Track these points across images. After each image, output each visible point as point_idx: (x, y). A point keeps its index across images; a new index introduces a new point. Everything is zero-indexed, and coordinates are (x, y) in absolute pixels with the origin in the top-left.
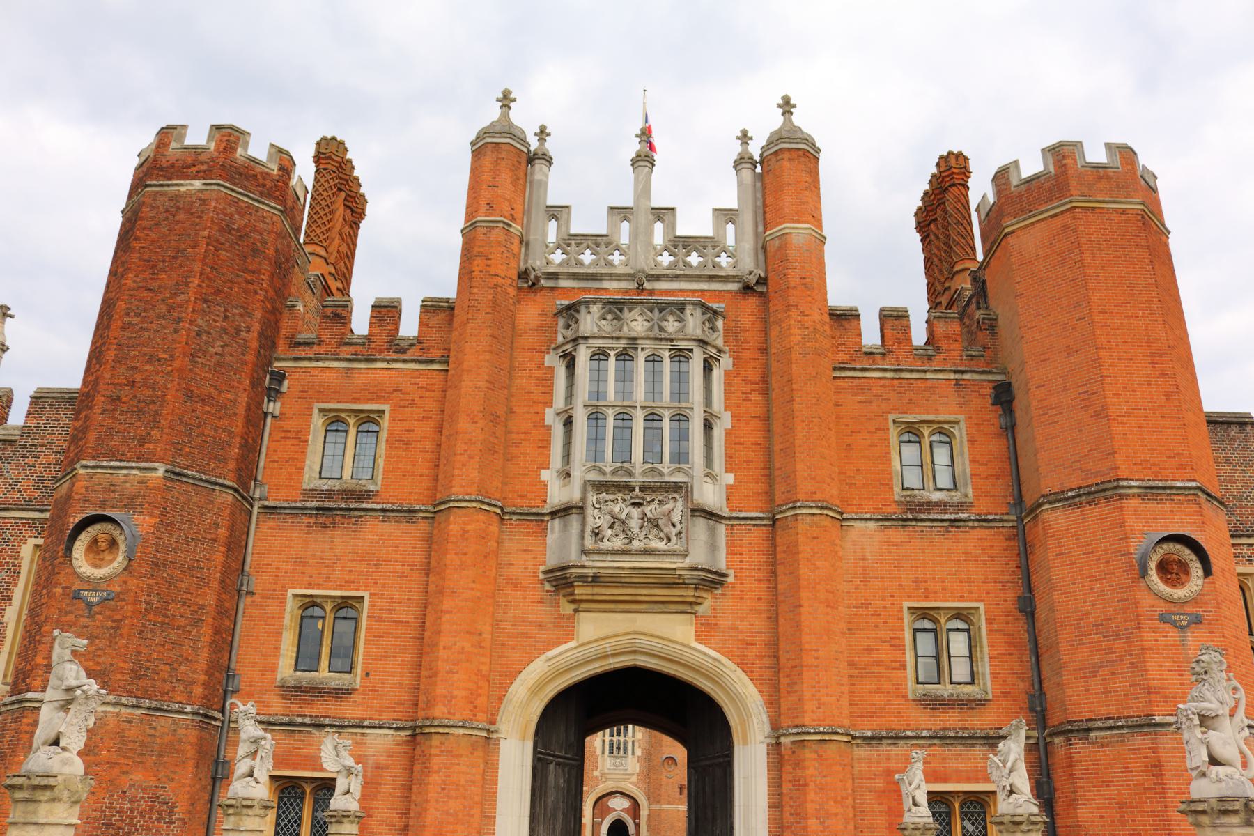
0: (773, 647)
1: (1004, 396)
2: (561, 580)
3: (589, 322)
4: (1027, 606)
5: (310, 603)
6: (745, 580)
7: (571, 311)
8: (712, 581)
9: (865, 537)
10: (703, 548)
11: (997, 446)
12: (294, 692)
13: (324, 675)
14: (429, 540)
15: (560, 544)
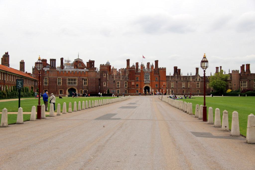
0: (151, 85)
1: (159, 76)
2: (145, 83)
3: (146, 74)
4: (159, 84)
5: (137, 85)
6: (151, 83)
7: (145, 73)
8: (150, 83)
9: (154, 81)
10: (149, 82)
11: (159, 78)
12: (137, 87)
13: (137, 87)
14: (141, 82)
15: (145, 82)
